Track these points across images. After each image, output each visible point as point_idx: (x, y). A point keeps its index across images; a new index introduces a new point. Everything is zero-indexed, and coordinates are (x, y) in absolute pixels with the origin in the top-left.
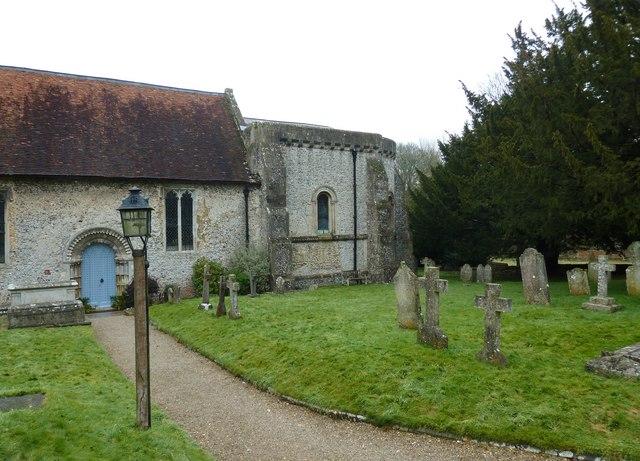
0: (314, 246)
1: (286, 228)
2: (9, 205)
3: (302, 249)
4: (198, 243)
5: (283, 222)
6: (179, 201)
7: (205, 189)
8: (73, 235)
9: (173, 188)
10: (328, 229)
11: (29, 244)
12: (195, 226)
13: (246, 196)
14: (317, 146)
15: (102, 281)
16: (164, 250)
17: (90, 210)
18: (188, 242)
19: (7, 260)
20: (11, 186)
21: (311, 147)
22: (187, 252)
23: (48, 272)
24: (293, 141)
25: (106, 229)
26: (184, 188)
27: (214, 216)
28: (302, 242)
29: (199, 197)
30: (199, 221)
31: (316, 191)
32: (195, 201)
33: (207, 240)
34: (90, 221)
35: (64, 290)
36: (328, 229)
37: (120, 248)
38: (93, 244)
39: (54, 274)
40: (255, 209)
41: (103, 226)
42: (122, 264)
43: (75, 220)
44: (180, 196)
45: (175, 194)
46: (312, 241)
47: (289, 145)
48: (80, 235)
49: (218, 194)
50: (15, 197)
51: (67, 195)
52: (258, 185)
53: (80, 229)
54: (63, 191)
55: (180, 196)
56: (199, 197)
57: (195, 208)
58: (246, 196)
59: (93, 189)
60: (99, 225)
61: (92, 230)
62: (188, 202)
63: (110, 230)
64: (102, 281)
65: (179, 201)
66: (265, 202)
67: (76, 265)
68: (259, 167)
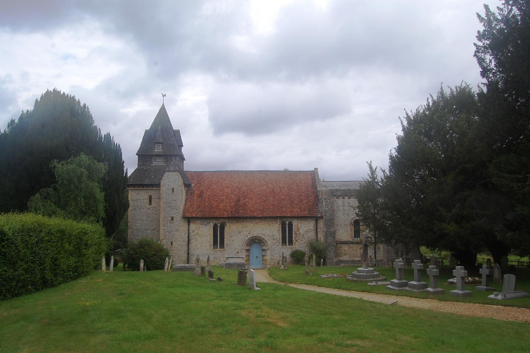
0: (351, 245)
1: (334, 237)
2: (226, 227)
3: (345, 247)
4: (295, 243)
5: (333, 234)
6: (287, 225)
7: (298, 220)
8: (247, 239)
9: (284, 220)
10: (359, 237)
11: (232, 241)
12: (294, 235)
13: (317, 222)
14: (352, 197)
15: (257, 257)
16: (281, 245)
17: (253, 229)
18: (291, 243)
19: (225, 248)
20: (226, 220)
21: (349, 198)
22: (291, 246)
23: (238, 253)
24: (340, 196)
25: (258, 237)
26: (289, 220)
27: (302, 231)
28: (345, 244)
29: (295, 223)
30: (295, 234)
31: (352, 219)
32: (294, 225)
33: (298, 242)
34: (253, 233)
35: (241, 258)
36: (359, 237)
38: (254, 242)
39: (240, 253)
40: (320, 228)
41: (258, 235)
42: (265, 251)
43: (247, 233)
44: (287, 223)
45: (286, 222)
46: (350, 243)
47: (338, 198)
48: (249, 239)
49: (303, 222)
50: (228, 224)
51: (245, 223)
52: (322, 217)
53: (249, 237)
54: (243, 222)
55: (287, 223)
56: (295, 223)
57: (294, 228)
58: (317, 222)
59: (254, 221)
60: (256, 235)
61: (253, 237)
62: (291, 225)
63: (260, 237)
64: (257, 257)
65: (287, 225)
66: (325, 226)
67: (248, 250)
68: (323, 207)
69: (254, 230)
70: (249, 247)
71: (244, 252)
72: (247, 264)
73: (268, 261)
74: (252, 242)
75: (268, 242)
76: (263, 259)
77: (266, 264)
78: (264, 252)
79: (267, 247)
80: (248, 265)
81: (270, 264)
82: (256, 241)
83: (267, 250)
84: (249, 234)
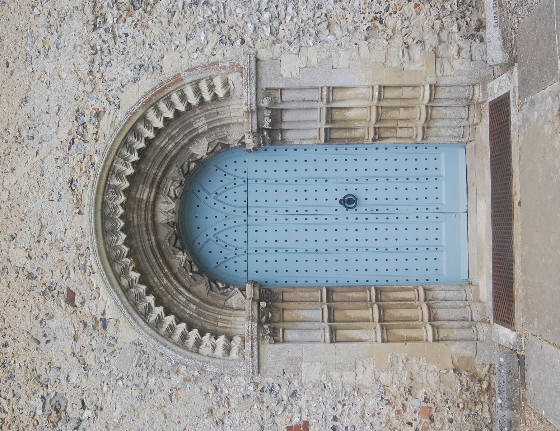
34: (70, 256)
37: (201, 124)
63: (111, 171)
69: (25, 240)
70: (236, 299)
71: (296, 362)
72: (432, 319)
73: (401, 69)
74: (182, 257)
75: (169, 73)
76: (378, 137)
77: (434, 87)
78: (287, 117)
79: (232, 77)
80: (441, 313)
81: (431, 40)
82: (162, 218)
83: (265, 84)
84: (70, 298)
